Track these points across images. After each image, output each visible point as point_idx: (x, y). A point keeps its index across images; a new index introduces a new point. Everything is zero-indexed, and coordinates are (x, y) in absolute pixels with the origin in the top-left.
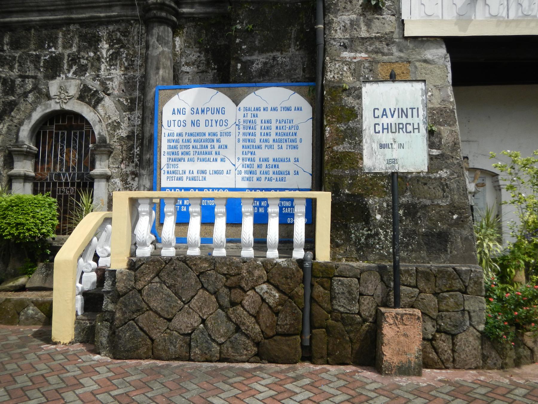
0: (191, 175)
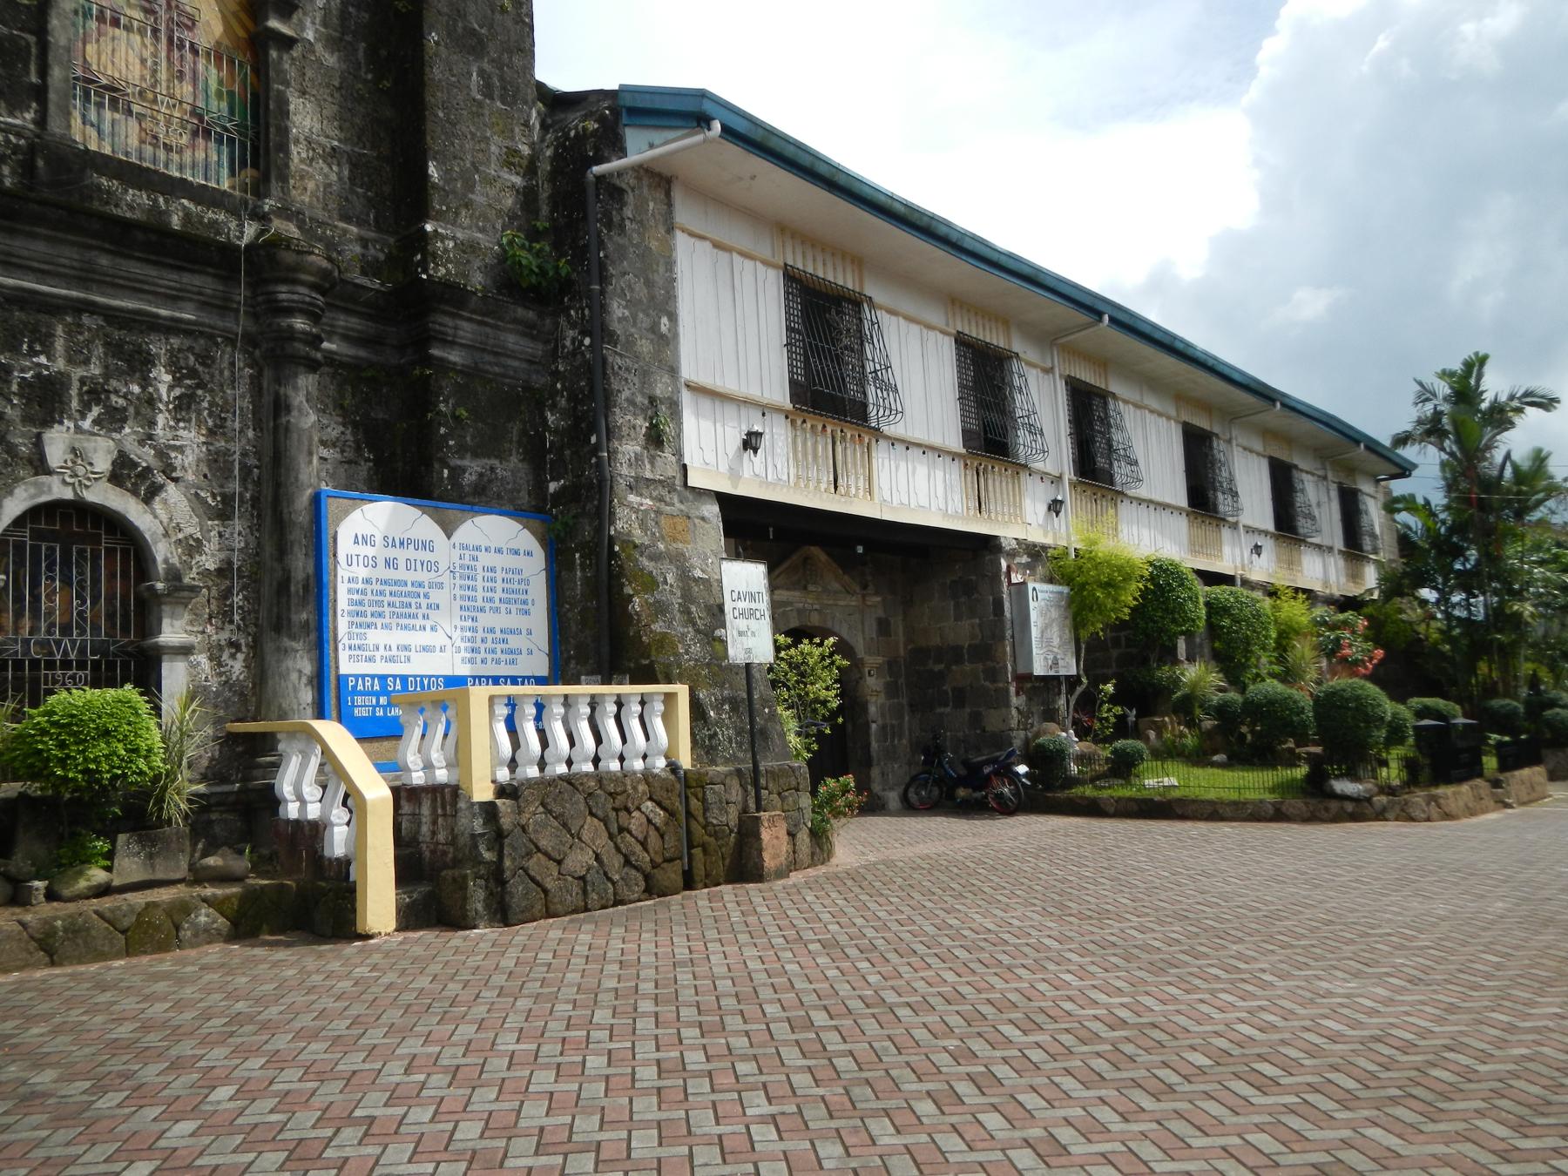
0: (388, 653)
